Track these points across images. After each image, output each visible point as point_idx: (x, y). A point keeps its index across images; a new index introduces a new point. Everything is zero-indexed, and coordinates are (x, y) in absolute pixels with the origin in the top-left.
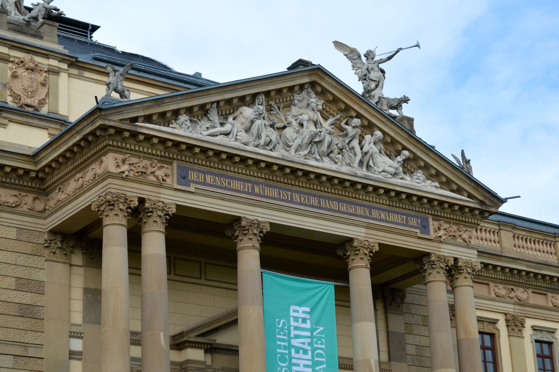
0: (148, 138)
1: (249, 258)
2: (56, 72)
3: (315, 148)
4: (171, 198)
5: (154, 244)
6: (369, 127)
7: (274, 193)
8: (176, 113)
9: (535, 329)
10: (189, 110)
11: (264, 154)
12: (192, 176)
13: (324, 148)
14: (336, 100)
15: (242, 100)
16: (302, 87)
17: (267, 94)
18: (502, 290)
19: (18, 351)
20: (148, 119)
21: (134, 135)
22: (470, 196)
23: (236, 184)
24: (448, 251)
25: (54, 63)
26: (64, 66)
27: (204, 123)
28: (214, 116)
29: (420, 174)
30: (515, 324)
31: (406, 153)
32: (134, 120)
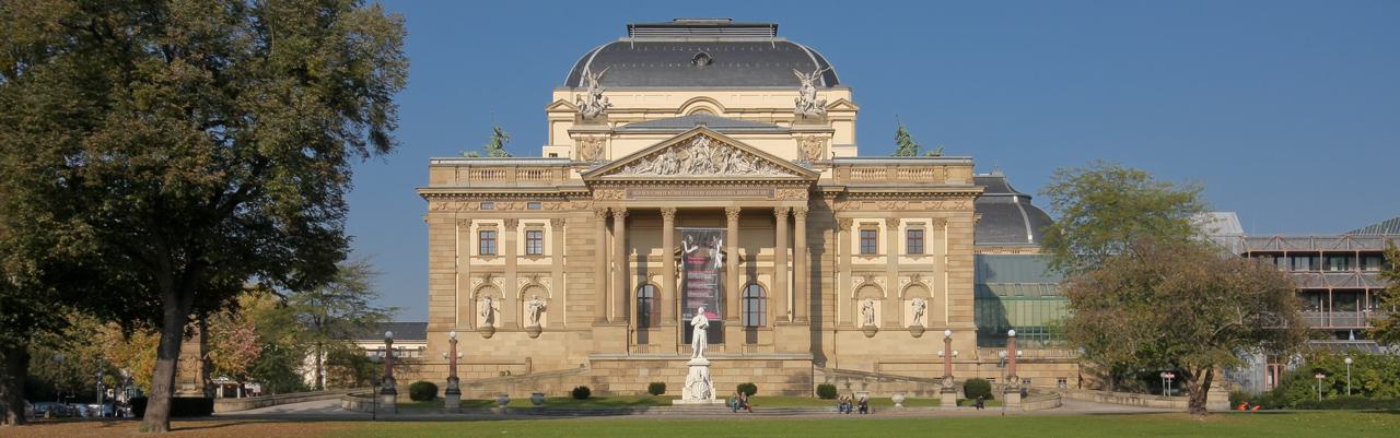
0: (608, 182)
1: (668, 225)
2: (604, 140)
5: (619, 225)
6: (736, 149)
7: (679, 193)
8: (623, 167)
9: (908, 224)
10: (630, 164)
11: (673, 176)
12: (634, 193)
13: (703, 167)
14: (714, 140)
15: (659, 153)
16: (694, 137)
17: (673, 146)
18: (884, 204)
19: (588, 270)
20: (608, 173)
21: (601, 182)
22: (799, 174)
23: (658, 193)
24: (787, 205)
27: (638, 168)
28: (644, 163)
29: (767, 168)
30: (892, 224)
32: (602, 174)
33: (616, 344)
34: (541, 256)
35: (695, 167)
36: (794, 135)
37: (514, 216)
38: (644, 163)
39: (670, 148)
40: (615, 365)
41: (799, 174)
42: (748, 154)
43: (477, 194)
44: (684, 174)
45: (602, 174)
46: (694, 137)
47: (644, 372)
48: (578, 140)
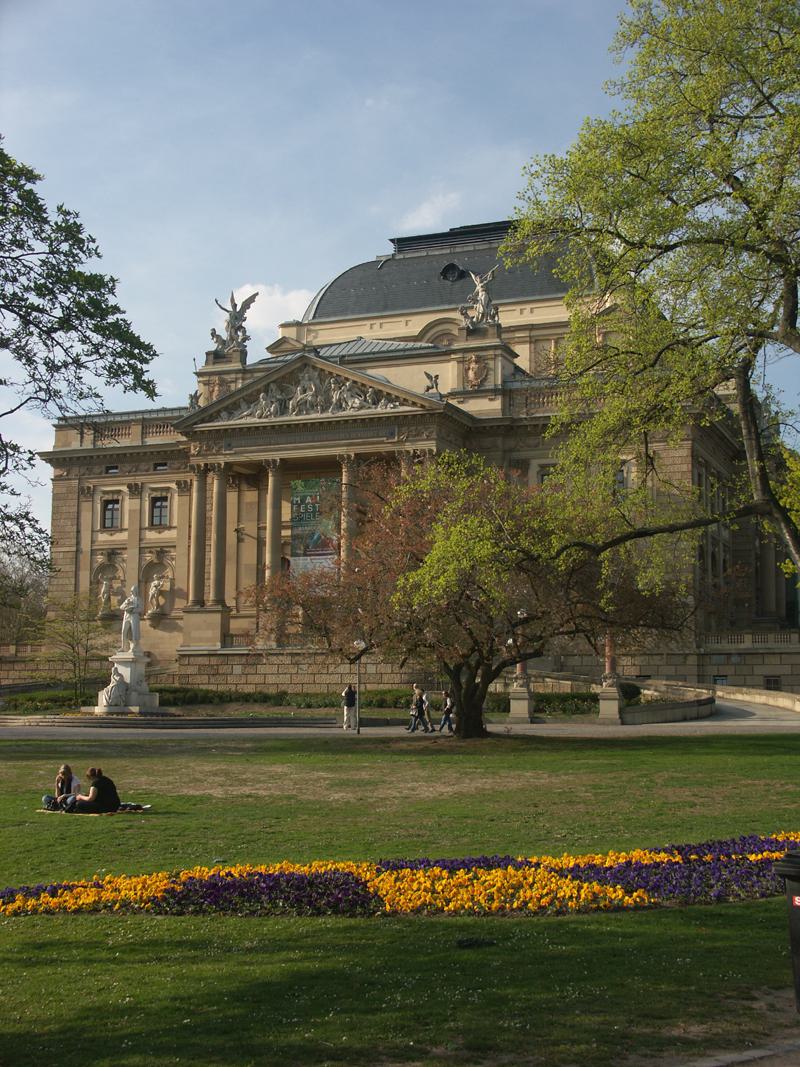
3: (303, 407)
4: (222, 460)
8: (219, 412)
10: (226, 409)
12: (233, 445)
14: (322, 370)
20: (203, 421)
22: (422, 406)
25: (233, 376)
26: (240, 375)
28: (244, 405)
31: (370, 390)
33: (209, 634)
34: (170, 528)
35: (302, 407)
36: (453, 356)
37: (139, 480)
38: (244, 405)
39: (273, 386)
40: (205, 661)
41: (422, 406)
42: (359, 389)
43: (98, 456)
44: (292, 417)
45: (196, 423)
46: (301, 370)
47: (238, 669)
48: (206, 384)
